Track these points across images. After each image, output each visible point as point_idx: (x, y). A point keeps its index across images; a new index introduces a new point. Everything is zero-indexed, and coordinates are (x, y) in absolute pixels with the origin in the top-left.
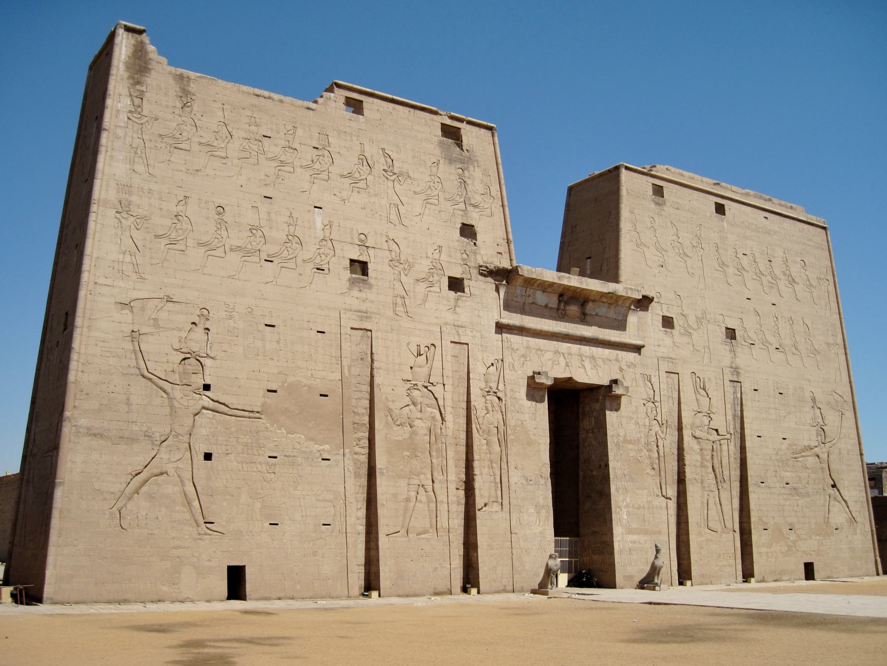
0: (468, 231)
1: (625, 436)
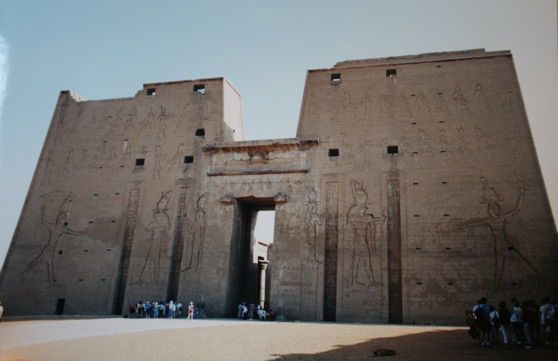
0: (201, 132)
1: (288, 225)
